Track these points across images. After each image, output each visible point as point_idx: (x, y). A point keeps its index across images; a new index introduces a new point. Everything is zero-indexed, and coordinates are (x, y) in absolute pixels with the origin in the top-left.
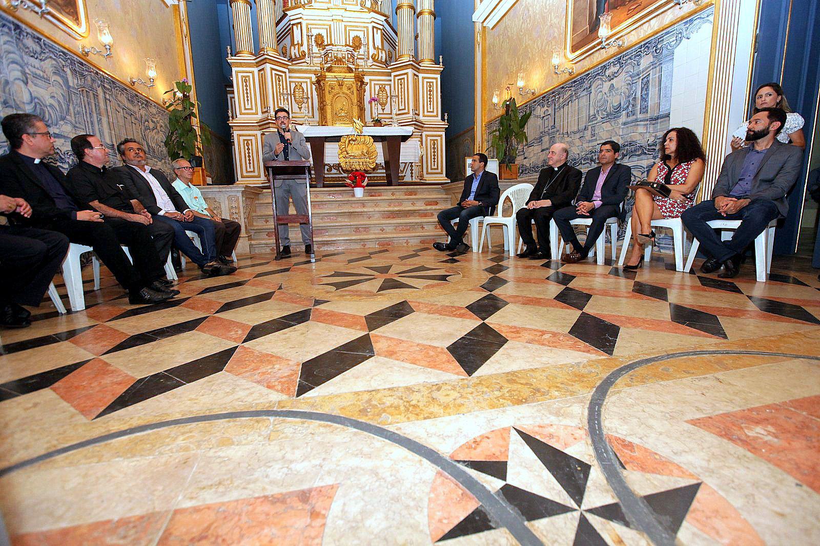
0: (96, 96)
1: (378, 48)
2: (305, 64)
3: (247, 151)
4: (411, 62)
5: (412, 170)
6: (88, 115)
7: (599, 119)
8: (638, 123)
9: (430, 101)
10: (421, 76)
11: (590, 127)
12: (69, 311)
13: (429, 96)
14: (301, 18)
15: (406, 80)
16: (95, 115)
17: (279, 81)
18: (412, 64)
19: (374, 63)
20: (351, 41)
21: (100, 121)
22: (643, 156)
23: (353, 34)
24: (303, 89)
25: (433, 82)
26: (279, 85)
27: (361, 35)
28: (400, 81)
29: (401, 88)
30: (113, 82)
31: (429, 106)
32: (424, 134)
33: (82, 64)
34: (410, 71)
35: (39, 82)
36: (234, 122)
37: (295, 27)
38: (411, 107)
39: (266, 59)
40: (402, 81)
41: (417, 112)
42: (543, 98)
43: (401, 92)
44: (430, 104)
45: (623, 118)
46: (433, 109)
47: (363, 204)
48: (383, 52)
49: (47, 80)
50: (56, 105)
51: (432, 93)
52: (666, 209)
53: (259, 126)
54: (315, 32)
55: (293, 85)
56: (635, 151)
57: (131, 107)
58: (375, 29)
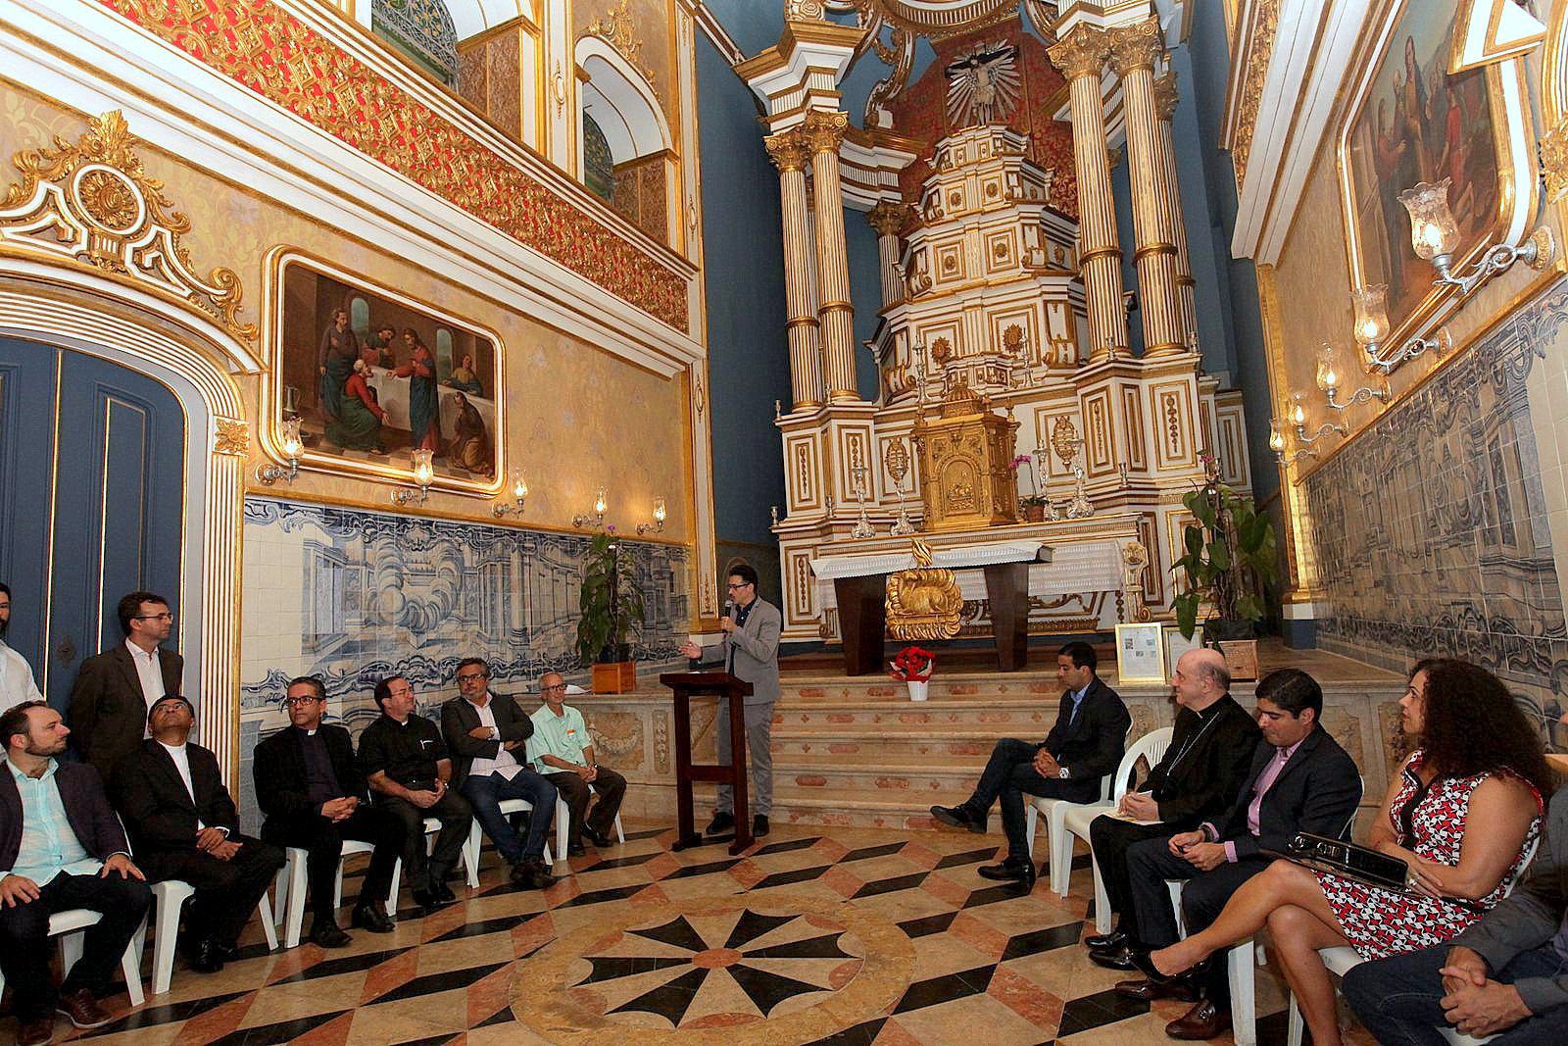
0: (506, 568)
1: (1061, 341)
2: (913, 401)
3: (799, 576)
4: (1112, 365)
5: (1120, 603)
6: (488, 599)
8: (1506, 568)
9: (1174, 435)
10: (1145, 384)
12: (282, 947)
14: (905, 320)
15: (1105, 400)
16: (500, 595)
17: (855, 446)
18: (1115, 368)
19: (1051, 372)
20: (1002, 339)
21: (507, 601)
23: (1004, 325)
24: (903, 448)
26: (855, 452)
27: (1021, 322)
29: (1098, 420)
30: (540, 536)
31: (1171, 445)
32: (1160, 511)
33: (490, 530)
34: (1113, 383)
35: (418, 579)
36: (781, 525)
37: (898, 337)
38: (1121, 458)
39: (830, 412)
41: (1140, 465)
43: (1098, 428)
44: (1175, 441)
45: (1478, 548)
46: (1183, 450)
47: (925, 715)
48: (1071, 346)
49: (431, 573)
50: (437, 599)
51: (1176, 416)
52: (1419, 918)
53: (821, 529)
54: (932, 338)
55: (886, 444)
57: (567, 560)
58: (1050, 307)
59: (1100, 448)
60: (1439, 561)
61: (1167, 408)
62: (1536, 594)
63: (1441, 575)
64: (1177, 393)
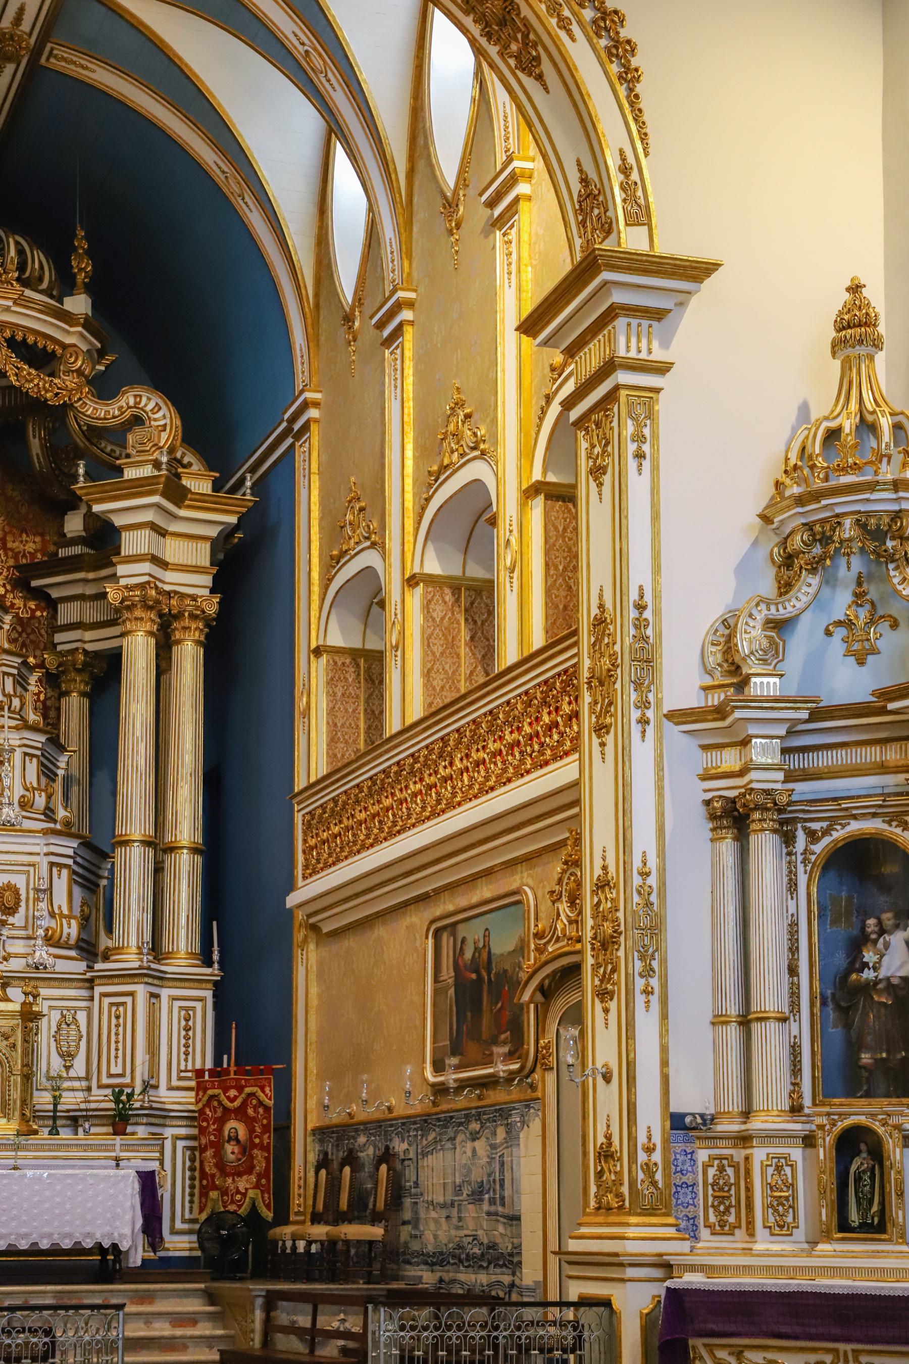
7: (465, 1195)
8: (499, 1218)
10: (165, 993)
11: (456, 1204)
13: (183, 1041)
22: (504, 1269)
25: (193, 1009)
28: (114, 1009)
29: (117, 1026)
40: (121, 1009)
42: (403, 1124)
45: (486, 1207)
51: (190, 1033)
56: (498, 1259)
59: (116, 1057)
60: (459, 1211)
61: (183, 1023)
62: (511, 1232)
63: (460, 1219)
64: (193, 1009)
